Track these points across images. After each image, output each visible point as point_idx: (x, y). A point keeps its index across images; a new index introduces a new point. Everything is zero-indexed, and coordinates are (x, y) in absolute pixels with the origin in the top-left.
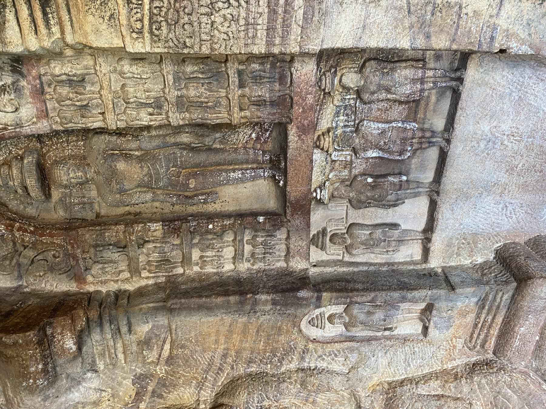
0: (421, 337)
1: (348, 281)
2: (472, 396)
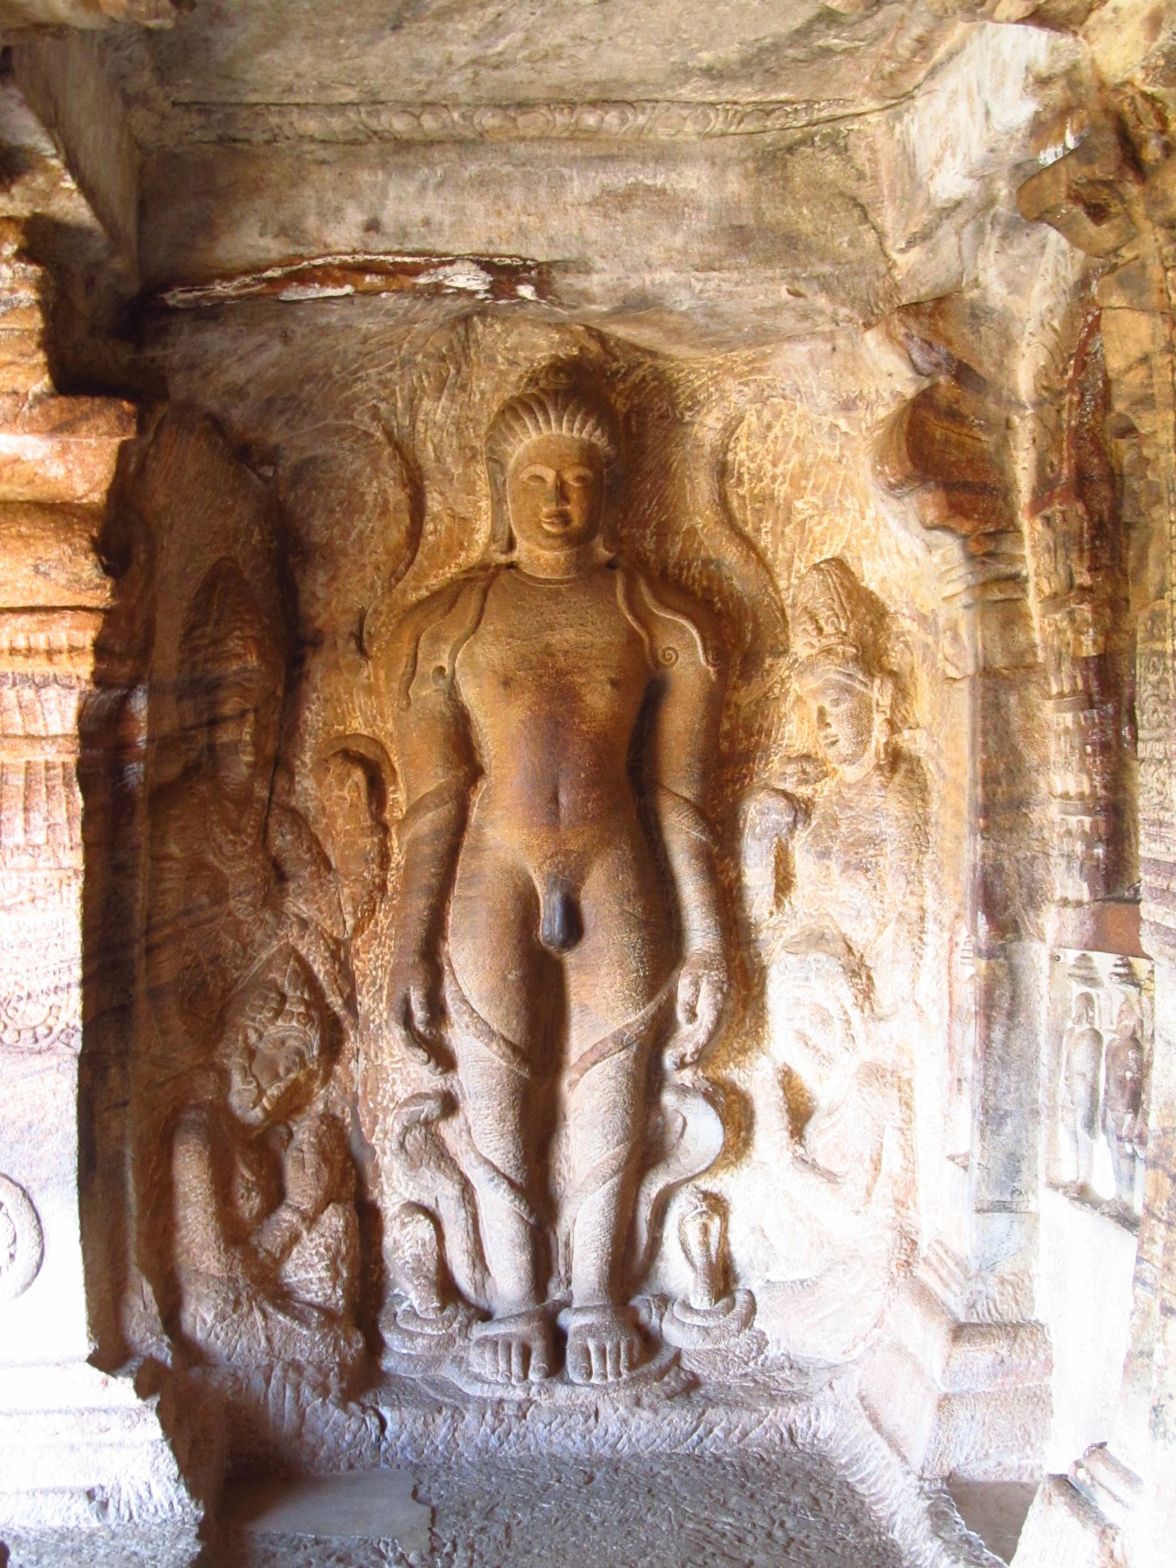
0: (951, 1151)
1: (1011, 1015)
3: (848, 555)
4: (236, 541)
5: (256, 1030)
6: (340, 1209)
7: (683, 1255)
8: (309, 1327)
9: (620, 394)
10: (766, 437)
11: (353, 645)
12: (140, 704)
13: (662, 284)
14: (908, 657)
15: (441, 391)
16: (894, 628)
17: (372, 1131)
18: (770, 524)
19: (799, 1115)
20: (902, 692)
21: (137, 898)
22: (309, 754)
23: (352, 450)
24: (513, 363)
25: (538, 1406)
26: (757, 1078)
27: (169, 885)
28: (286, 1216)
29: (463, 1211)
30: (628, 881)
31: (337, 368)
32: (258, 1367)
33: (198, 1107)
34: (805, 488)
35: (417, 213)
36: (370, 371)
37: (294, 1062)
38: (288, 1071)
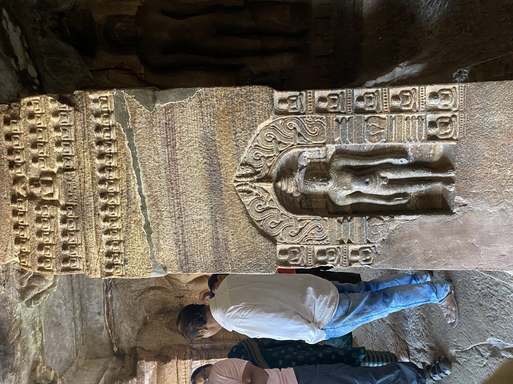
35: (96, 305)
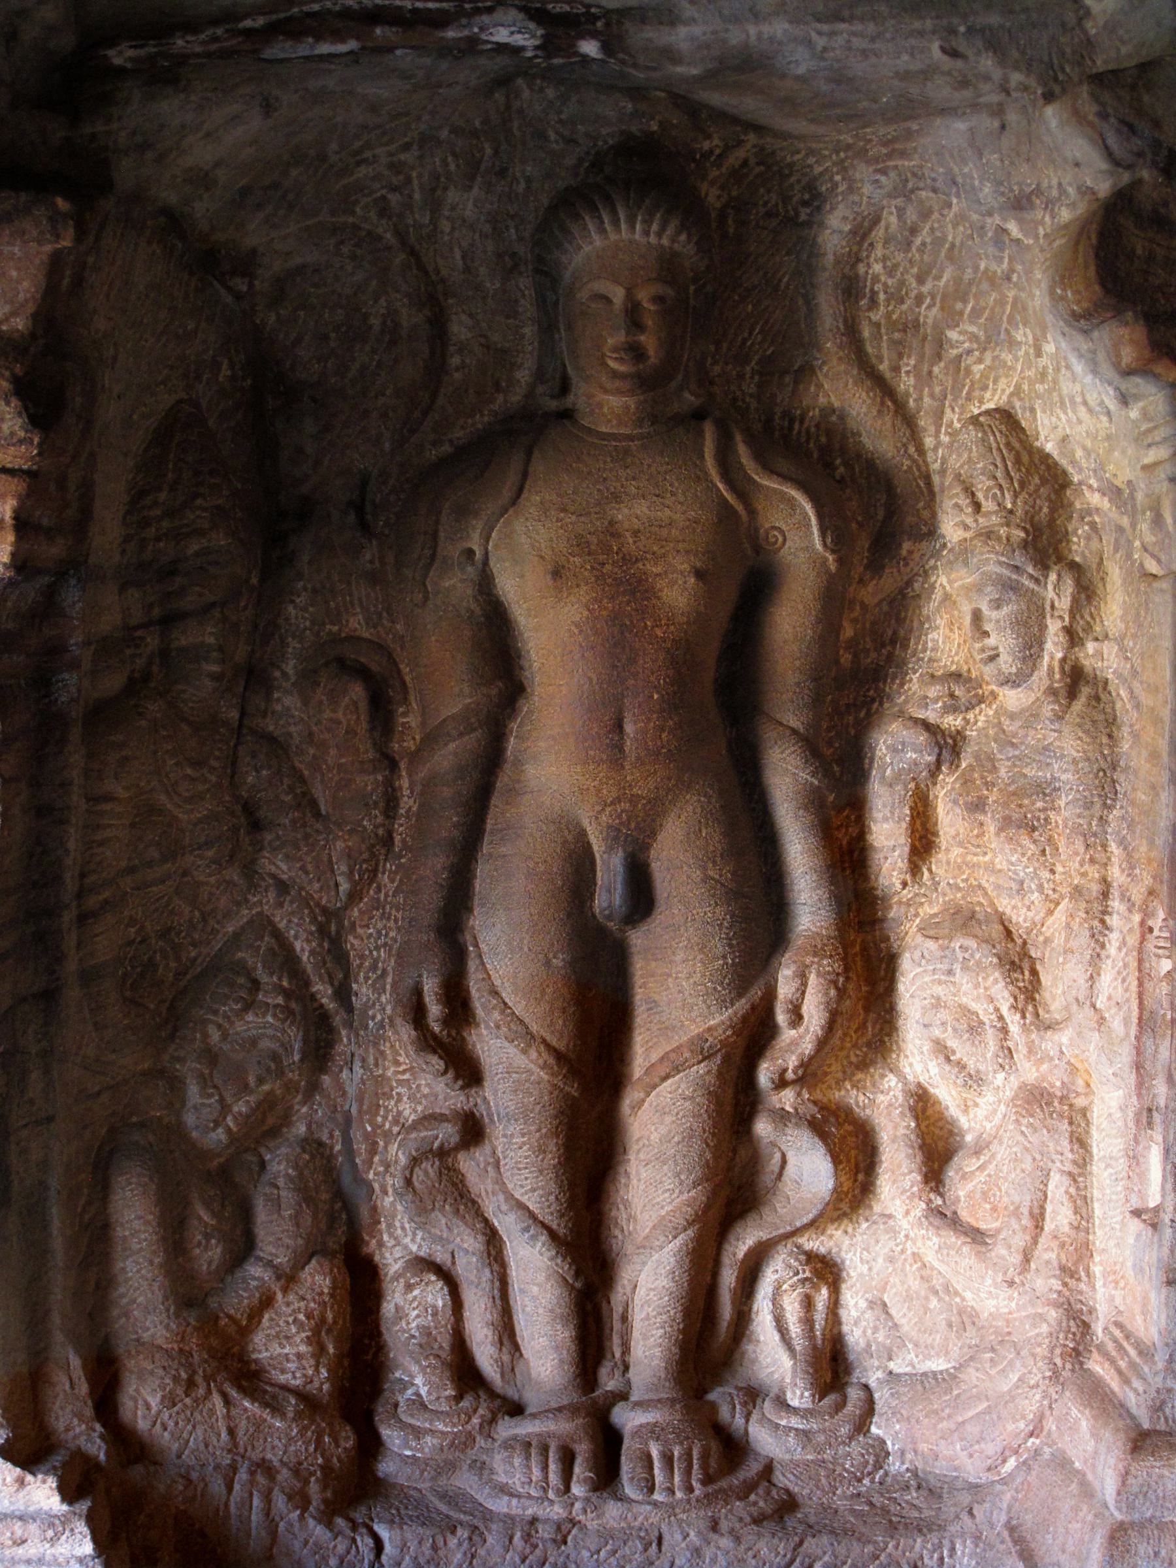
0: (1135, 1202)
2: (1026, 1293)
3: (1018, 404)
4: (198, 377)
5: (219, 1026)
6: (327, 1263)
7: (777, 1337)
8: (283, 1416)
9: (712, 183)
10: (909, 244)
11: (352, 518)
12: (72, 598)
13: (772, 40)
14: (1095, 544)
15: (472, 178)
16: (1078, 505)
17: (370, 1163)
18: (912, 362)
19: (937, 1151)
20: (1087, 590)
21: (67, 851)
22: (292, 662)
23: (353, 257)
24: (571, 141)
25: (583, 1528)
26: (883, 1103)
27: (108, 833)
28: (256, 1272)
29: (487, 1272)
30: (713, 836)
31: (334, 146)
32: (217, 1467)
33: (142, 1125)
34: (961, 313)
36: (379, 151)
37: (268, 1070)
38: (261, 1081)
